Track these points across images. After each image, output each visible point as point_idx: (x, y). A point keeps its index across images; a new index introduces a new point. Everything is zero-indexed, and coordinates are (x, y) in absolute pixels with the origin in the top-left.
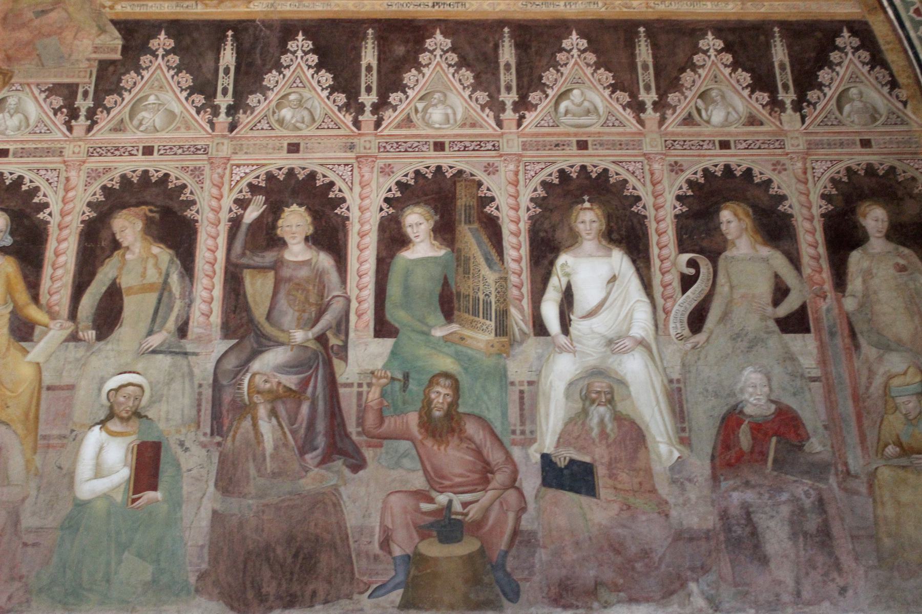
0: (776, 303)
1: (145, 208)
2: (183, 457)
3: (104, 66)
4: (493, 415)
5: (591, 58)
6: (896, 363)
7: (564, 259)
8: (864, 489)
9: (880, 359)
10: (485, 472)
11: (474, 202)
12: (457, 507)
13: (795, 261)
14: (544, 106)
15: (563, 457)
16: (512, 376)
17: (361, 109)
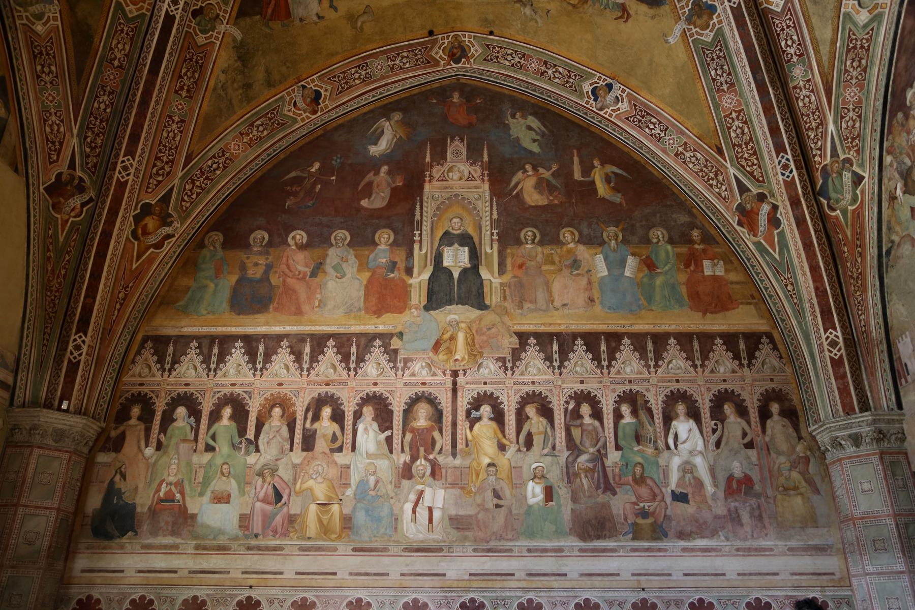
0: (743, 438)
1: (535, 404)
2: (559, 491)
3: (514, 350)
4: (655, 477)
5: (678, 347)
6: (782, 459)
7: (674, 423)
8: (772, 502)
9: (777, 458)
10: (654, 496)
11: (643, 402)
12: (647, 508)
13: (749, 423)
14: (664, 366)
15: (678, 491)
16: (660, 464)
17: (602, 367)
